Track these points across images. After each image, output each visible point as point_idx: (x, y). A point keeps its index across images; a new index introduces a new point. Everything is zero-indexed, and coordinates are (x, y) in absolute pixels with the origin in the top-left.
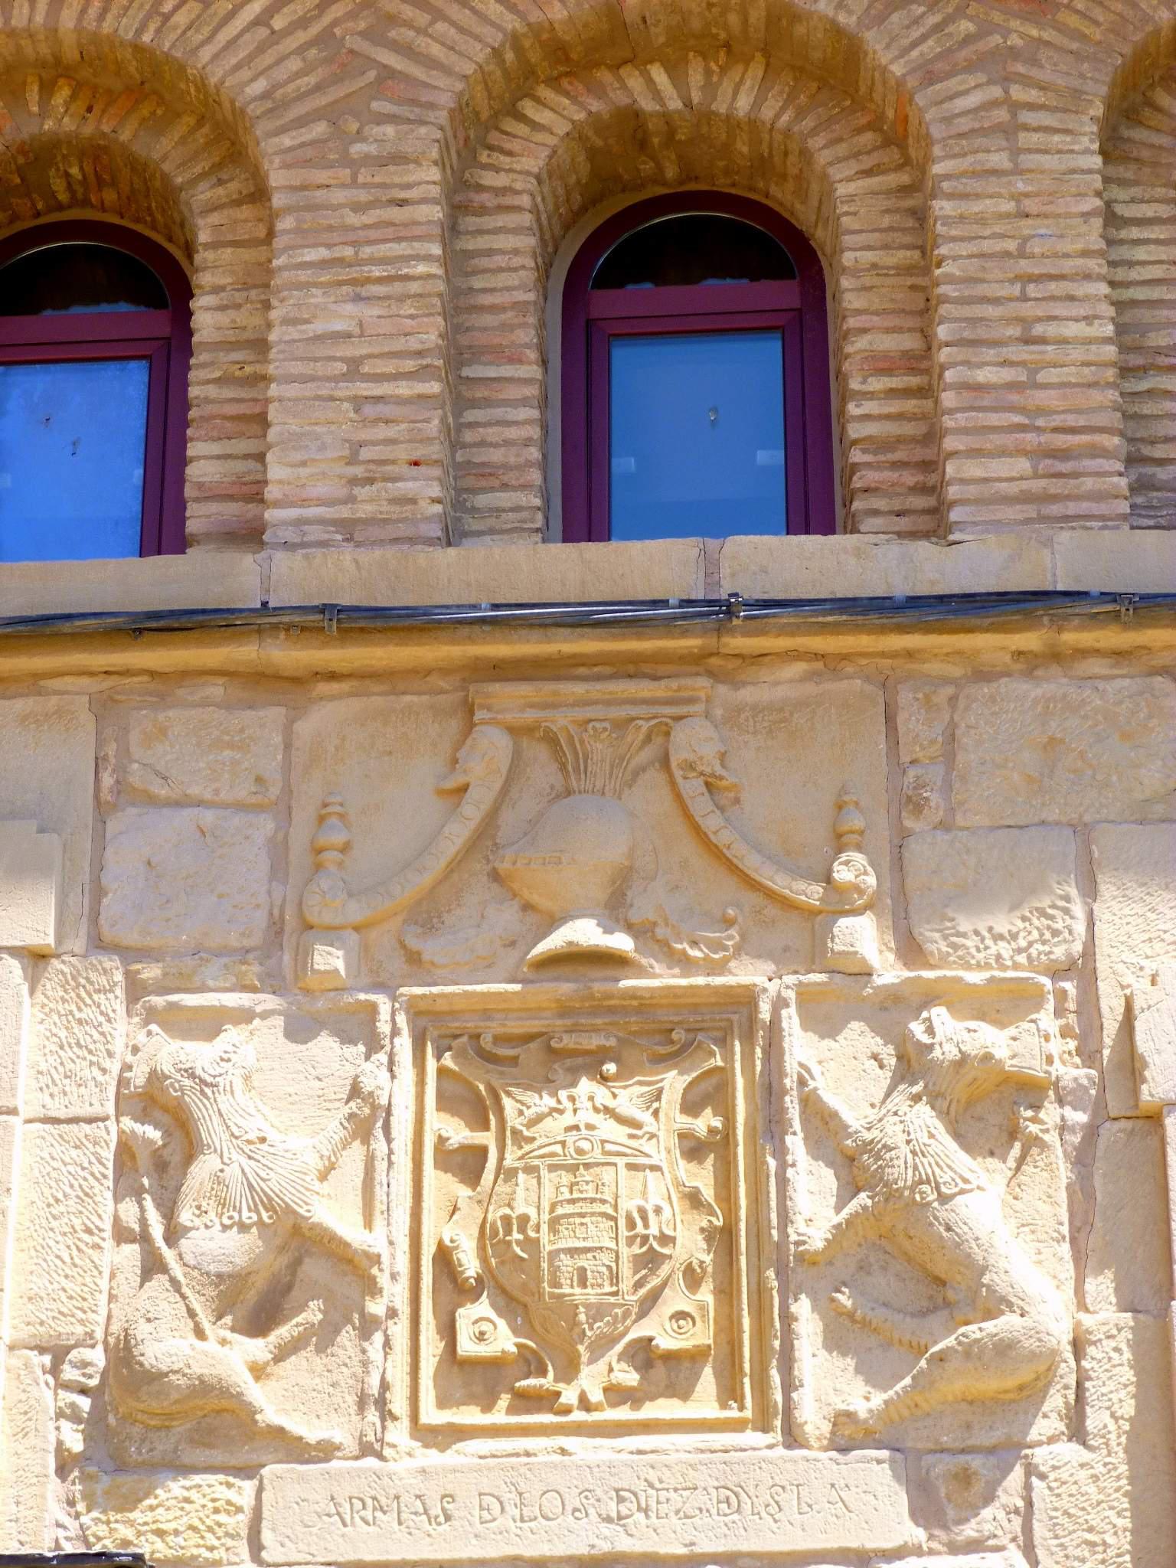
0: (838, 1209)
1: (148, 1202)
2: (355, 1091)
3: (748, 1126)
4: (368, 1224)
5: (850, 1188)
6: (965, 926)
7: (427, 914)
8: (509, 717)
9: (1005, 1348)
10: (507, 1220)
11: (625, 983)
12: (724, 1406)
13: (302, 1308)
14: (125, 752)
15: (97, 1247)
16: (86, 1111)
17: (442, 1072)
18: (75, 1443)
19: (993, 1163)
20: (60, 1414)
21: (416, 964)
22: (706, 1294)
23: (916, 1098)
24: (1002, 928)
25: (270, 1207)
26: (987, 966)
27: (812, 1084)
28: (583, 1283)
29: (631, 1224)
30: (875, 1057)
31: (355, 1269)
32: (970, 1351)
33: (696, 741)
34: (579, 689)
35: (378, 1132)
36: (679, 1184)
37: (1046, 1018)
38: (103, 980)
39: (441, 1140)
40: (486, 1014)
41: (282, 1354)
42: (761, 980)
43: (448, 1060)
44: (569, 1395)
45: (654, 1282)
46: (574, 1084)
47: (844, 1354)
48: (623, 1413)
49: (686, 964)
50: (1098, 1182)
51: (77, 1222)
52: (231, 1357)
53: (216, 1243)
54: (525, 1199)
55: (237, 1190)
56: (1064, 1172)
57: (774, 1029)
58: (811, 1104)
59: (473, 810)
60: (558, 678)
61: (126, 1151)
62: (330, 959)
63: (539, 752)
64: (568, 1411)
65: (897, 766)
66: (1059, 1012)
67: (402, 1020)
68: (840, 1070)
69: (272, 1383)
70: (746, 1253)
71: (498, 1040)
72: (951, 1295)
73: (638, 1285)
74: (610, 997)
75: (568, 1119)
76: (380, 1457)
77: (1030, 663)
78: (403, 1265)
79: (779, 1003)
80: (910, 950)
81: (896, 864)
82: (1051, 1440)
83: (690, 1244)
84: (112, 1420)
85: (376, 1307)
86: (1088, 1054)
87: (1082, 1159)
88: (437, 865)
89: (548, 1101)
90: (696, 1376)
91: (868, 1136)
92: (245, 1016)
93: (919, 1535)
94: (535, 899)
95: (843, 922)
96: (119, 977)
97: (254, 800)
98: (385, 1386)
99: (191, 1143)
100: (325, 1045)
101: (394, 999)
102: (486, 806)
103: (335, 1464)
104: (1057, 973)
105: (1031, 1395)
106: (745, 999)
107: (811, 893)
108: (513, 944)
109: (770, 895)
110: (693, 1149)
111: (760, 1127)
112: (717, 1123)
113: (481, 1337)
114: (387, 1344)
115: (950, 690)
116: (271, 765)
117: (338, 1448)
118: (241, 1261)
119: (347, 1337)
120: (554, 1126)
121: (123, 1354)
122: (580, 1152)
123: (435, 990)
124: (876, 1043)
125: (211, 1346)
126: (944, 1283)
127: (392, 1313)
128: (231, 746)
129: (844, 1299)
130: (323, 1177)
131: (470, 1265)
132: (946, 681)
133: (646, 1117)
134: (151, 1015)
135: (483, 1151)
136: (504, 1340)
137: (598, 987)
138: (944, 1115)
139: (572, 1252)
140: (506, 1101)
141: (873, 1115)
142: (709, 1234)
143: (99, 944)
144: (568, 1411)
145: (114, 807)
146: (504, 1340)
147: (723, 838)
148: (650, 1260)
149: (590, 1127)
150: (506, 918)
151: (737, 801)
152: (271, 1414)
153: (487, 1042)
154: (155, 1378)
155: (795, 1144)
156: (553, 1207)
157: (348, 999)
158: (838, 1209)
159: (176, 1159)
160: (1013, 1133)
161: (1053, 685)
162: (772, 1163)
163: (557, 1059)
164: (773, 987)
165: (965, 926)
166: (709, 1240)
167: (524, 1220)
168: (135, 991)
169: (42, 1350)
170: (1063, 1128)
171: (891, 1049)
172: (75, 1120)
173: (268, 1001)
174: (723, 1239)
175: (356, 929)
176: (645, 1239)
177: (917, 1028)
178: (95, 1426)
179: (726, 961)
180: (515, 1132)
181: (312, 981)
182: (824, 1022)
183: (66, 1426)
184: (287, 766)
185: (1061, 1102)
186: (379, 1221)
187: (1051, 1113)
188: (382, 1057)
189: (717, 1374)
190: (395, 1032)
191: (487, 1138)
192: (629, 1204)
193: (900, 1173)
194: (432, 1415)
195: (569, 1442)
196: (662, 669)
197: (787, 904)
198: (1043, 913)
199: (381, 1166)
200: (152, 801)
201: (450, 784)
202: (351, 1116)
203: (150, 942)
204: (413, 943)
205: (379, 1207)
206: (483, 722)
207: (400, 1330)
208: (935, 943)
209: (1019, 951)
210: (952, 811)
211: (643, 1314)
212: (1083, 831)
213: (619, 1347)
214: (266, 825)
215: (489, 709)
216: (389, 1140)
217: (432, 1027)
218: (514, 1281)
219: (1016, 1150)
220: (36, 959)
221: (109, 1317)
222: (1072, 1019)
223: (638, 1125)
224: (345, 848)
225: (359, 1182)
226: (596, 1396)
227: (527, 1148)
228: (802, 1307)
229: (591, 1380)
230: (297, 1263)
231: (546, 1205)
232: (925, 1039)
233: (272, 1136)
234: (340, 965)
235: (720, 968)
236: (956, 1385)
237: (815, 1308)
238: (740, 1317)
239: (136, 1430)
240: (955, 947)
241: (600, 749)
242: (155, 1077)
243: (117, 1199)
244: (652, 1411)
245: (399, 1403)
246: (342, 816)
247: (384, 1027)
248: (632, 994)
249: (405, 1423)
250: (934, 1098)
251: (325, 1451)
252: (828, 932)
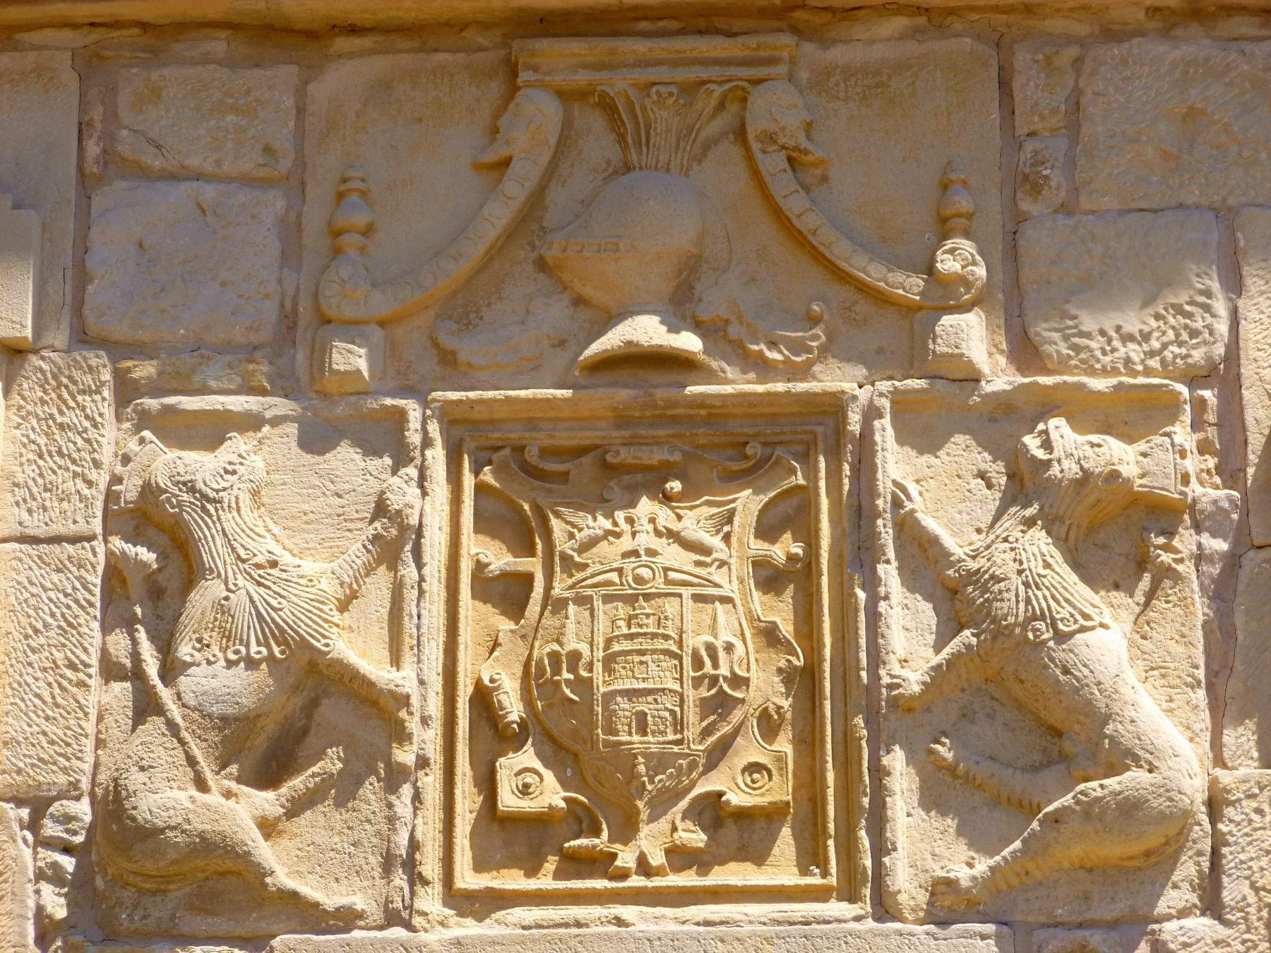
0: (938, 648)
1: (142, 635)
2: (381, 509)
3: (836, 548)
4: (396, 661)
5: (949, 627)
6: (1089, 324)
7: (463, 307)
8: (558, 79)
9: (1130, 808)
10: (555, 657)
11: (692, 390)
12: (804, 871)
13: (319, 755)
14: (112, 116)
15: (81, 684)
16: (72, 529)
17: (480, 489)
18: (58, 907)
19: (1118, 597)
20: (40, 876)
21: (451, 367)
22: (784, 744)
23: (1029, 523)
24: (1132, 327)
25: (282, 640)
26: (1115, 372)
27: (909, 506)
28: (643, 730)
29: (698, 663)
30: (982, 475)
31: (381, 712)
32: (1089, 811)
33: (778, 108)
34: (641, 47)
35: (407, 556)
36: (752, 618)
37: (1182, 433)
38: (88, 379)
39: (480, 566)
40: (532, 424)
41: (295, 808)
42: (849, 387)
43: (487, 476)
44: (626, 858)
45: (726, 729)
46: (633, 504)
47: (944, 814)
48: (688, 879)
49: (764, 368)
50: (1239, 620)
51: (58, 655)
52: (238, 810)
53: (217, 679)
54: (576, 634)
55: (244, 619)
56: (1200, 608)
57: (865, 442)
58: (908, 529)
59: (516, 188)
60: (616, 34)
61: (115, 574)
62: (352, 358)
63: (596, 121)
64: (623, 875)
65: (1012, 140)
66: (1197, 425)
67: (434, 428)
68: (943, 491)
69: (285, 842)
70: (831, 698)
71: (545, 453)
72: (1068, 746)
73: (706, 732)
74: (674, 404)
75: (626, 543)
76: (409, 927)
78: (435, 707)
79: (872, 413)
80: (1025, 352)
81: (1008, 252)
82: (1183, 913)
83: (766, 687)
84: (99, 883)
85: (405, 756)
86: (1229, 473)
87: (1221, 593)
88: (475, 251)
89: (604, 523)
90: (772, 838)
91: (973, 565)
92: (251, 423)
94: (588, 291)
95: (947, 320)
96: (106, 376)
97: (262, 173)
98: (414, 845)
99: (190, 567)
100: (346, 457)
101: (425, 404)
102: (530, 185)
103: (356, 934)
104: (1195, 379)
105: (1159, 863)
106: (835, 406)
107: (911, 286)
108: (562, 343)
109: (863, 289)
110: (770, 578)
111: (848, 556)
112: (797, 549)
113: (525, 790)
114: (417, 798)
115: (1074, 51)
116: (282, 132)
117: (360, 915)
118: (248, 701)
119: (370, 790)
120: (609, 551)
121: (112, 805)
122: (639, 580)
123: (472, 395)
124: (983, 459)
125: (214, 798)
126: (1059, 734)
127: (423, 762)
128: (235, 109)
129: (944, 751)
130: (343, 607)
131: (513, 708)
132: (1070, 40)
133: (716, 542)
134: (144, 420)
135: (528, 578)
137: (661, 394)
138: (1061, 542)
139: (631, 694)
140: (555, 523)
141: (979, 541)
142: (788, 676)
143: (83, 338)
144: (623, 875)
145: (101, 180)
147: (808, 222)
148: (719, 705)
149: (652, 553)
150: (555, 314)
151: (825, 179)
152: (283, 878)
153: (532, 455)
154: (150, 834)
155: (889, 573)
156: (608, 642)
157: (372, 404)
158: (938, 648)
159: (173, 585)
160: (1142, 562)
162: (861, 595)
163: (612, 476)
164: (864, 394)
165: (1089, 324)
166: (787, 682)
167: (575, 657)
168: (126, 391)
169: (19, 802)
170: (1200, 557)
171: (1000, 466)
172: (56, 540)
173: (278, 406)
174: (803, 682)
175: (382, 324)
176: (714, 680)
177: (1032, 442)
178: (79, 889)
179: (809, 364)
180: (565, 558)
181: (331, 385)
182: (922, 433)
183: (47, 889)
184: (300, 134)
185: (1198, 528)
186: (408, 657)
187: (1186, 541)
188: (412, 471)
189: (796, 836)
190: (427, 443)
191: (534, 565)
192: (696, 641)
193: (1011, 607)
194: (467, 879)
195: (628, 912)
196: (738, 25)
197: (881, 299)
198: (1179, 310)
199: (411, 595)
200: (144, 173)
201: (490, 157)
202: (376, 538)
203: (144, 336)
204: (447, 341)
205: (408, 641)
206: (529, 85)
207: (431, 782)
208: (1055, 344)
209: (1152, 354)
210: (1075, 191)
211: (711, 766)
212: (1225, 216)
213: (684, 803)
214: (275, 203)
215: (536, 69)
216: (420, 565)
217: (468, 437)
218: (564, 726)
219: (1145, 582)
221: (96, 766)
222: (1212, 432)
223: (706, 551)
224: (368, 231)
225: (385, 612)
226: (657, 858)
227: (579, 576)
228: (896, 760)
229: (651, 841)
230: (313, 704)
231: (600, 640)
232: (1041, 454)
233: (285, 558)
234: (363, 365)
235: (803, 372)
236: (1074, 849)
237: (910, 761)
238: (823, 771)
239: (128, 895)
240: (1077, 349)
241: (665, 119)
242: (149, 491)
243: (106, 630)
244: (723, 876)
245: (430, 866)
246: (364, 194)
247: (415, 438)
248: (701, 402)
249: (438, 888)
250: (1051, 522)
251: (346, 919)
252: (929, 331)
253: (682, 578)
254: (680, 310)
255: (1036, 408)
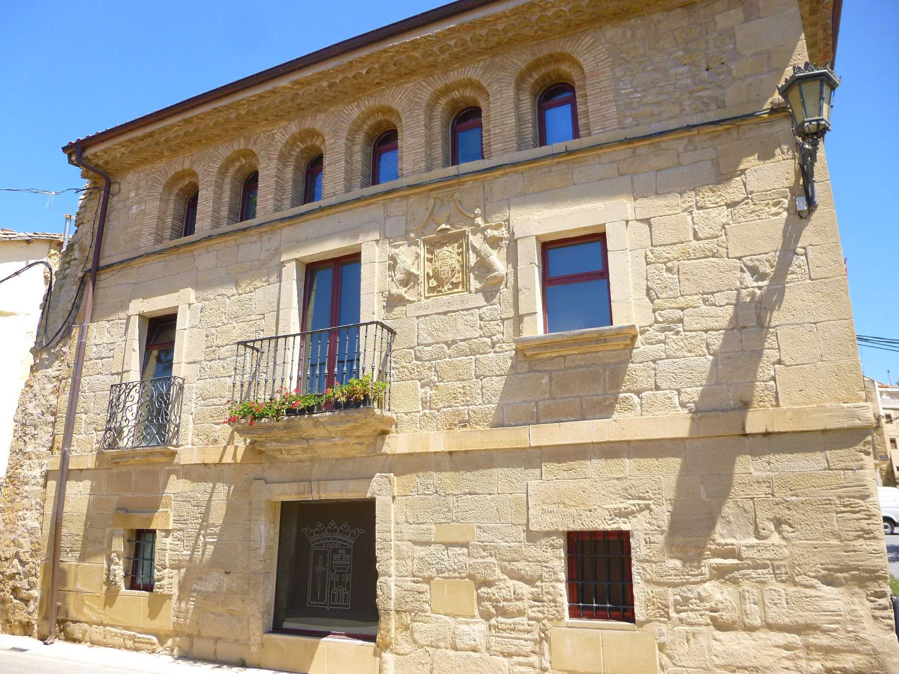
3: (466, 248)
7: (424, 227)
9: (495, 277)
21: (424, 235)
31: (416, 277)
32: (491, 278)
33: (457, 196)
37: (503, 229)
49: (457, 228)
52: (402, 291)
53: (399, 276)
54: (437, 264)
58: (472, 246)
59: (429, 211)
62: (412, 235)
68: (476, 240)
70: (465, 268)
77: (502, 175)
80: (486, 221)
83: (458, 267)
86: (509, 233)
87: (508, 248)
93: (485, 303)
105: (500, 283)
106: (465, 231)
110: (459, 254)
131: (431, 274)
136: (435, 284)
143: (385, 237)
146: (435, 284)
148: (453, 271)
150: (434, 225)
152: (407, 298)
155: (470, 252)
161: (506, 178)
168: (390, 243)
174: (462, 266)
178: (387, 302)
182: (474, 234)
187: (504, 242)
193: (483, 254)
194: (427, 295)
217: (425, 242)
220: (377, 241)
228: (471, 274)
229: (446, 288)
236: (490, 282)
241: (446, 199)
251: (414, 301)
253: (449, 255)
254: (447, 222)
255: (487, 228)
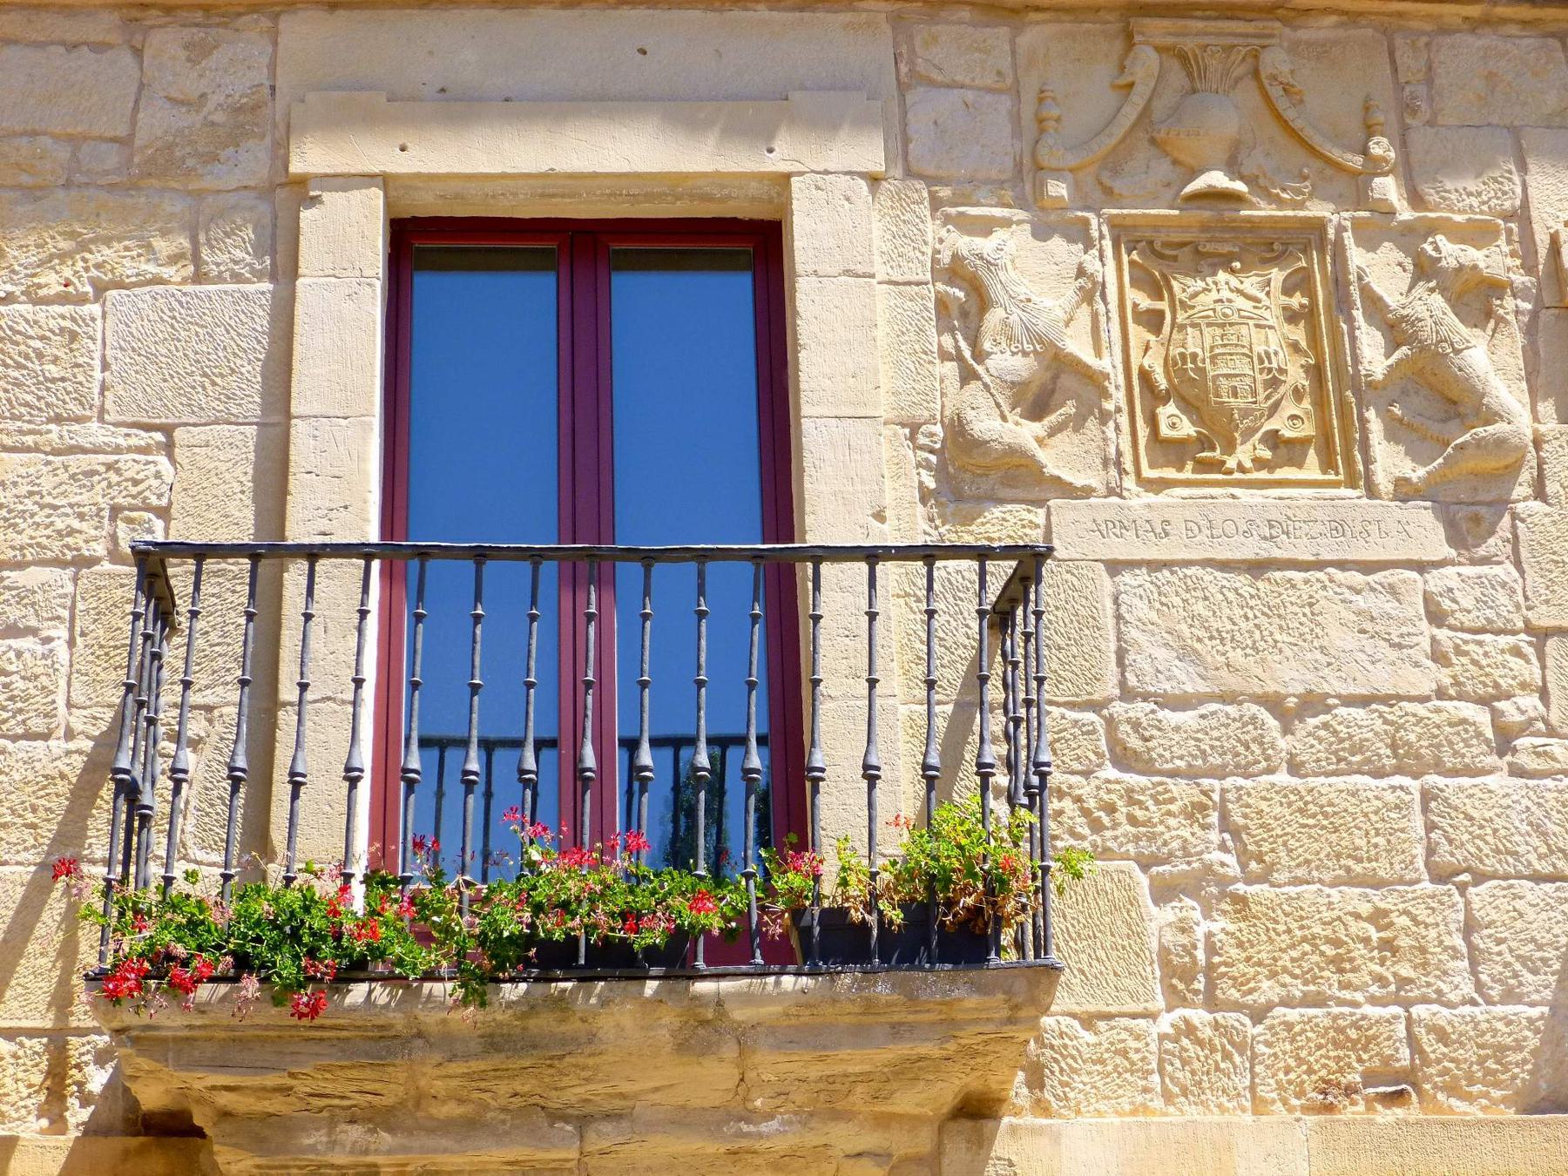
0: (1387, 356)
1: (959, 337)
2: (1081, 272)
3: (1327, 304)
4: (1098, 354)
5: (1392, 345)
6: (1449, 185)
7: (1114, 163)
8: (1158, 41)
9: (1500, 442)
10: (1183, 355)
11: (1243, 213)
12: (1324, 472)
13: (1062, 405)
14: (912, 51)
15: (930, 362)
16: (914, 278)
17: (1132, 263)
18: (931, 483)
19: (1477, 331)
20: (919, 465)
22: (1306, 404)
23: (1432, 290)
24: (1472, 188)
25: (1041, 342)
26: (1464, 212)
27: (1367, 279)
28: (1235, 395)
29: (1261, 361)
30: (1400, 264)
31: (1094, 381)
32: (1479, 443)
34: (1200, 25)
35: (1098, 298)
36: (1286, 338)
38: (916, 196)
39: (1135, 305)
40: (1156, 228)
41: (1053, 431)
42: (1327, 214)
43: (1135, 256)
44: (1231, 463)
45: (1276, 397)
46: (1214, 274)
47: (1397, 443)
48: (1263, 475)
49: (1280, 203)
50: (1541, 343)
51: (917, 347)
52: (1024, 433)
53: (1006, 363)
55: (1018, 330)
56: (1520, 339)
57: (1339, 246)
59: (1138, 99)
60: (1184, 17)
61: (942, 304)
62: (1058, 189)
63: (1175, 64)
64: (1230, 472)
65: (1399, 87)
66: (1509, 242)
67: (1105, 229)
68: (1381, 270)
69: (1048, 450)
70: (1331, 380)
71: (1165, 244)
72: (1462, 410)
73: (1268, 398)
74: (1234, 221)
75: (1214, 295)
76: (1121, 496)
77: (1474, 25)
78: (1121, 380)
79: (1340, 229)
80: (1416, 200)
81: (1403, 144)
82: (1526, 499)
83: (1296, 375)
84: (951, 470)
85: (1109, 406)
86: (1529, 268)
87: (1530, 330)
88: (1119, 131)
89: (1200, 284)
90: (1305, 454)
91: (1405, 312)
92: (1006, 223)
93: (1453, 553)
94: (1182, 157)
95: (1377, 180)
96: (925, 194)
97: (998, 86)
98: (1119, 454)
99: (982, 300)
100: (1057, 244)
101: (1099, 216)
102: (1146, 97)
103: (1092, 500)
104: (1508, 217)
105: (1513, 470)
106: (1319, 225)
107: (1356, 162)
108: (1168, 185)
109: (1329, 161)
110: (1292, 317)
111: (1334, 303)
112: (1305, 301)
113: (1173, 426)
114: (1117, 428)
115: (1424, 39)
116: (1005, 64)
117: (1094, 490)
118: (1025, 374)
119: (1092, 423)
120: (1207, 299)
121: (957, 429)
122: (1225, 315)
123: (1125, 211)
124: (1400, 256)
125: (1010, 425)
126: (1455, 403)
127: (1118, 410)
128: (978, 50)
129: (1397, 410)
130: (1067, 325)
131: (1163, 383)
132: (1424, 33)
133: (1262, 296)
134: (947, 219)
135: (1161, 314)
136: (1187, 429)
137: (1228, 215)
138: (1448, 301)
139: (1227, 376)
140: (1174, 283)
141: (1403, 300)
142: (1307, 369)
143: (909, 173)
144: (1230, 472)
145: (909, 87)
146: (1187, 429)
147: (1297, 124)
149: (1230, 301)
150: (1163, 168)
151: (1302, 101)
152: (1051, 469)
153: (1158, 246)
154: (981, 444)
155: (1358, 314)
156: (1212, 348)
157: (1070, 215)
158: (1387, 356)
159: (974, 310)
160: (1489, 314)
161: (1487, 40)
162: (1345, 327)
163: (1204, 258)
164: (1335, 218)
165: (1449, 185)
166: (1306, 372)
167: (1194, 356)
168: (936, 204)
169: (903, 425)
170: (1517, 312)
171: (1409, 260)
172: (909, 283)
173: (1019, 214)
175: (1071, 171)
176: (1270, 370)
177: (1428, 248)
178: (940, 472)
179: (1304, 201)
180: (1181, 302)
181: (1047, 203)
183: (923, 472)
184: (1014, 65)
185: (1515, 296)
186: (1105, 353)
187: (1510, 303)
188: (1095, 252)
189: (1318, 453)
190: (1102, 237)
191: (1164, 305)
192: (1259, 349)
193: (1427, 333)
194: (1147, 472)
195: (1237, 491)
196: (1249, 15)
197: (1339, 167)
198: (1495, 180)
199: (1103, 319)
200: (931, 83)
201: (1123, 81)
202: (1081, 288)
203: (941, 173)
204: (1108, 182)
205: (1105, 344)
206: (1141, 43)
207: (1124, 420)
208: (1433, 197)
209: (1484, 203)
210: (1435, 115)
211: (1270, 416)
212: (1515, 132)
213: (1259, 435)
214: (1005, 103)
215: (1143, 34)
216: (1106, 304)
217: (1124, 235)
218: (1190, 393)
219: (1492, 324)
220: (874, 180)
221: (943, 406)
222: (1517, 246)
223: (1259, 301)
224: (1058, 120)
225: (1089, 329)
226: (1248, 464)
227: (1190, 312)
229: (1243, 454)
230: (1055, 378)
231: (1207, 346)
232: (1434, 254)
233: (1034, 298)
234: (1065, 193)
235: (1300, 205)
236: (1470, 464)
237: (1378, 415)
238: (1331, 420)
239: (967, 476)
240: (1444, 199)
241: (1214, 64)
242: (956, 257)
243: (940, 334)
244: (1280, 474)
245: (1128, 464)
246: (1054, 99)
247: (1095, 234)
248: (1249, 219)
249: (1133, 476)
250: (1443, 290)
251: (1087, 492)
252: (1368, 186)
253: (1243, 318)
255: (1431, 229)
